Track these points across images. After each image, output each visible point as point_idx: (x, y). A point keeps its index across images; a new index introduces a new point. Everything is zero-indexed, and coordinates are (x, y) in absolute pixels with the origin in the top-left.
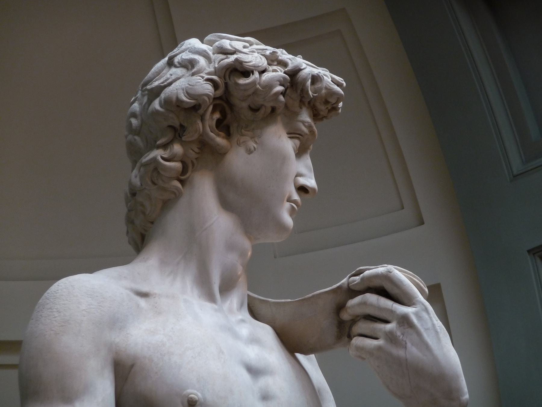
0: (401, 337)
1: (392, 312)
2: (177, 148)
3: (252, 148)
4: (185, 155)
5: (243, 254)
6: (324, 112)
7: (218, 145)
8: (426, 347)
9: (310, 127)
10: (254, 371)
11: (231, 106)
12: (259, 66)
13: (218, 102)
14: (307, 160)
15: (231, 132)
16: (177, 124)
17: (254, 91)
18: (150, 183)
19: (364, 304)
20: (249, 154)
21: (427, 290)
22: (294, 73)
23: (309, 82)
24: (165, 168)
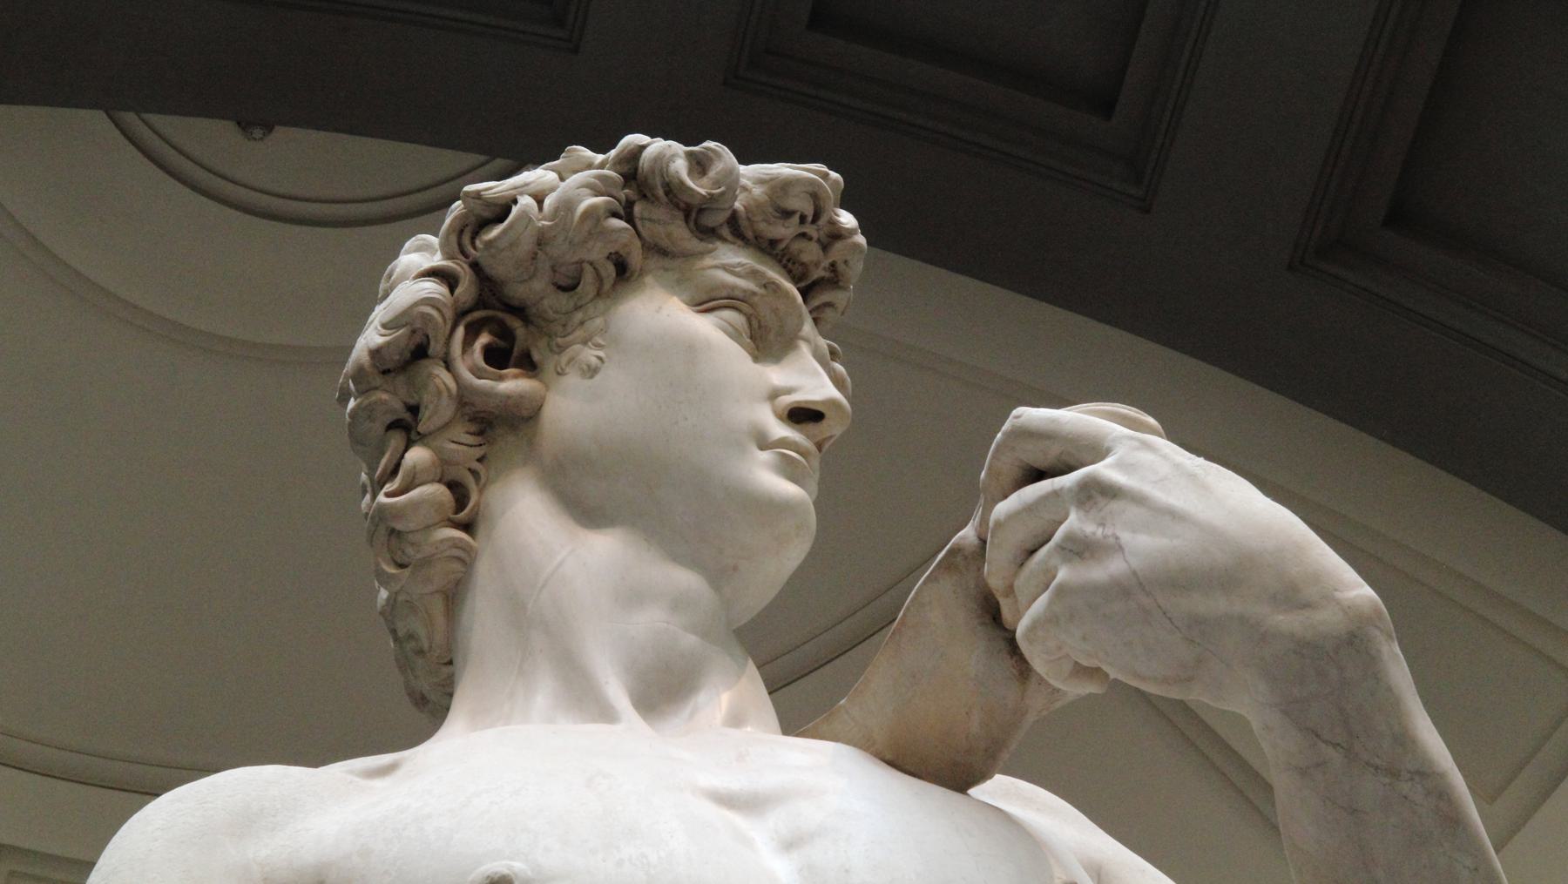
0: (1100, 531)
1: (1056, 494)
2: (417, 455)
3: (594, 361)
5: (678, 603)
7: (509, 397)
8: (1174, 515)
11: (519, 311)
12: (527, 185)
13: (477, 315)
15: (536, 356)
18: (392, 570)
20: (592, 377)
21: (1151, 421)
23: (680, 166)
24: (398, 513)
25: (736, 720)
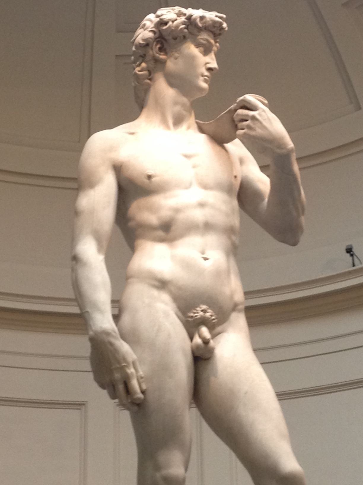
1: (247, 115)
2: (144, 65)
4: (147, 67)
5: (183, 105)
6: (218, 32)
9: (207, 40)
10: (187, 156)
11: (165, 40)
13: (159, 39)
14: (212, 55)
15: (167, 51)
16: (142, 54)
17: (171, 31)
18: (137, 84)
19: (238, 115)
21: (266, 102)
22: (189, 18)
23: (198, 20)
25: (189, 128)
